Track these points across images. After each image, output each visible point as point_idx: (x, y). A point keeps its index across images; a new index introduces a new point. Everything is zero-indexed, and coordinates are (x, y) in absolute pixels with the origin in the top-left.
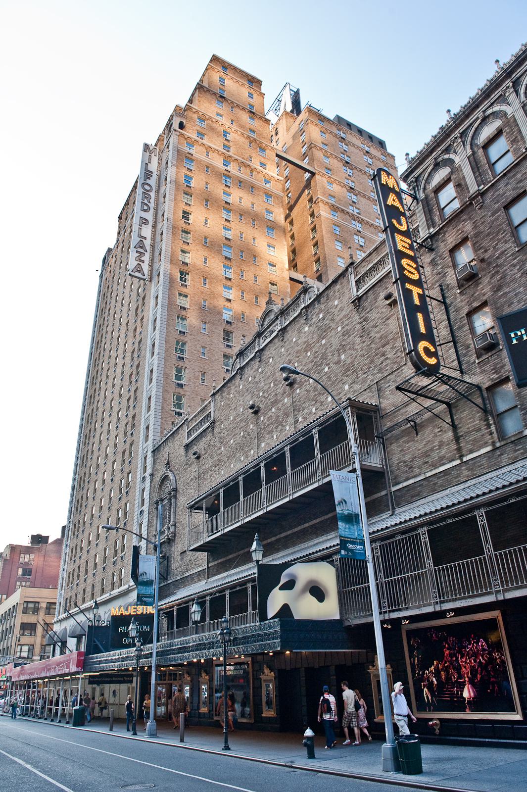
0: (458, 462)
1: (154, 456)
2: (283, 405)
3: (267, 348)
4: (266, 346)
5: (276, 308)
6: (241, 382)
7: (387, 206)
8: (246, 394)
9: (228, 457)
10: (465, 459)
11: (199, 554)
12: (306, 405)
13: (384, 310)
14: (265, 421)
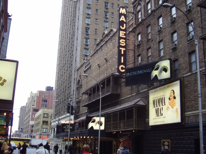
0: (131, 95)
1: (77, 72)
2: (105, 67)
4: (103, 45)
5: (106, 32)
7: (119, 21)
10: (132, 95)
11: (84, 108)
12: (109, 69)
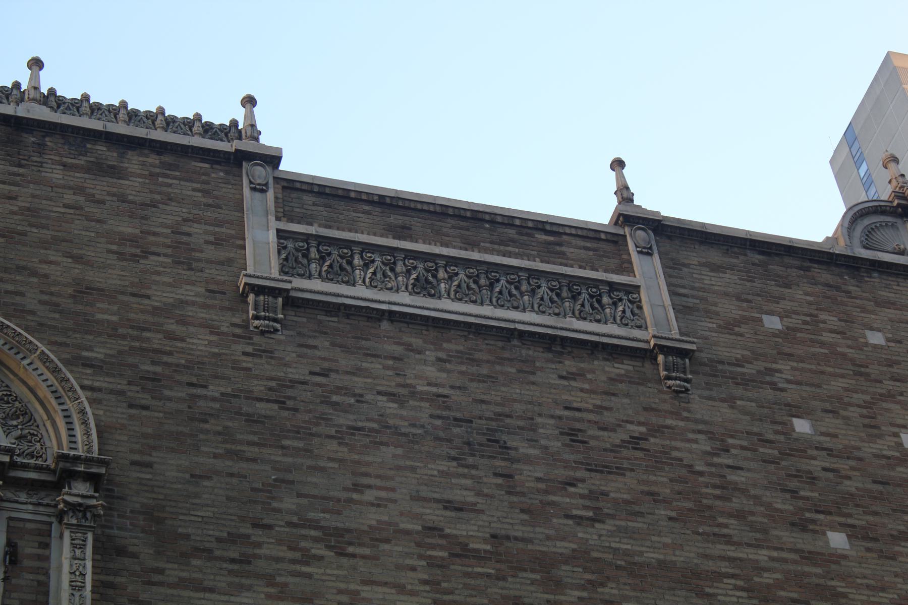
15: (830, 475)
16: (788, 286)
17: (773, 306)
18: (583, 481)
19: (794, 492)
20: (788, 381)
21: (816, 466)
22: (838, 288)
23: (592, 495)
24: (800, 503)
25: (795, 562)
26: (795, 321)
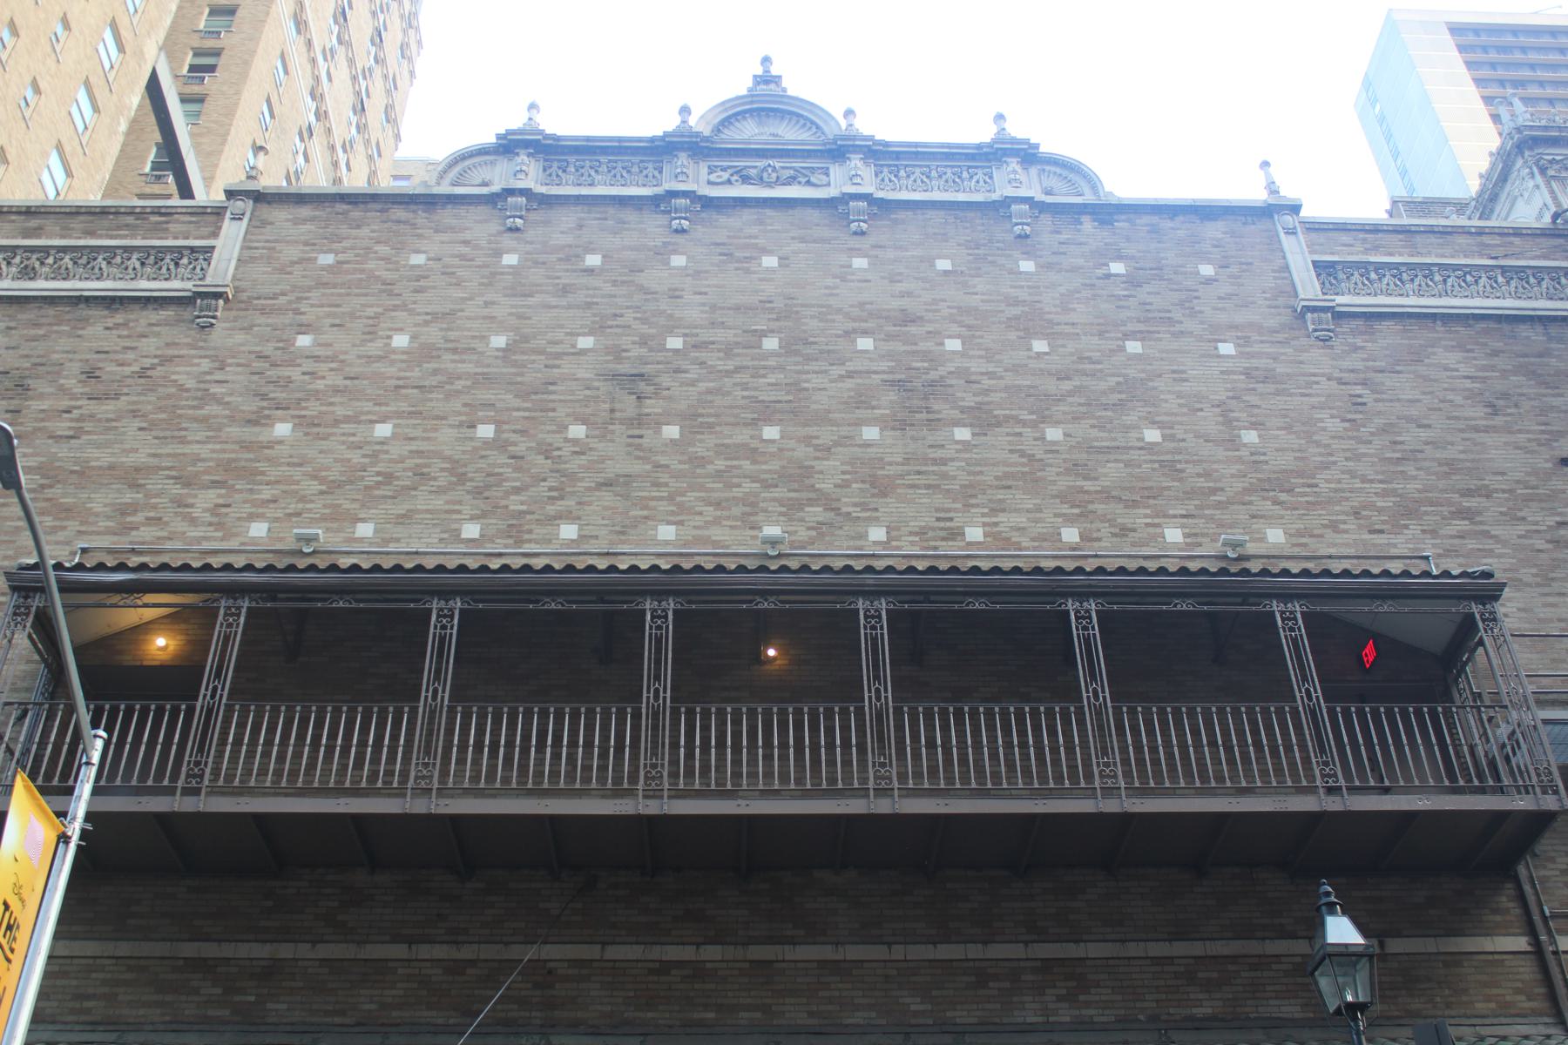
3: (747, 215)
4: (742, 202)
6: (508, 240)
8: (553, 301)
9: (333, 487)
13: (1459, 399)
14: (699, 450)
15: (307, 377)
16: (358, 227)
17: (335, 246)
18: (80, 407)
19: (264, 397)
20: (312, 306)
21: (295, 373)
22: (405, 223)
23: (80, 419)
24: (265, 404)
25: (233, 451)
26: (349, 256)
